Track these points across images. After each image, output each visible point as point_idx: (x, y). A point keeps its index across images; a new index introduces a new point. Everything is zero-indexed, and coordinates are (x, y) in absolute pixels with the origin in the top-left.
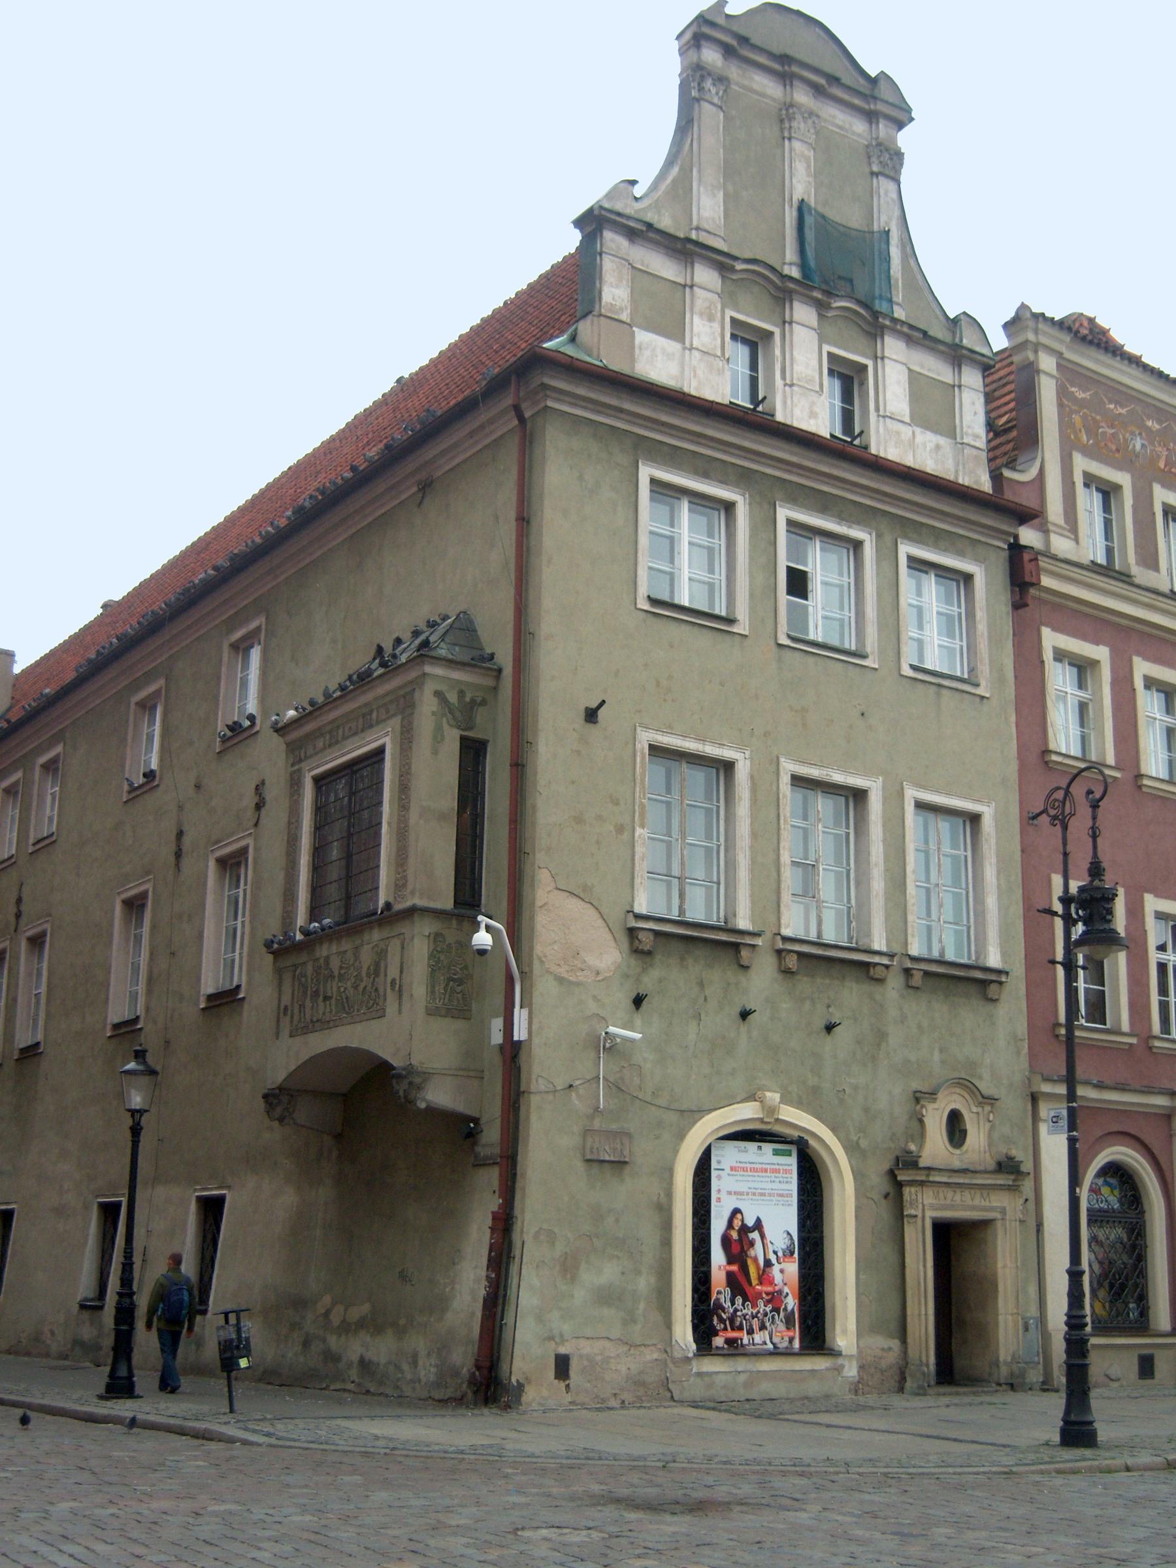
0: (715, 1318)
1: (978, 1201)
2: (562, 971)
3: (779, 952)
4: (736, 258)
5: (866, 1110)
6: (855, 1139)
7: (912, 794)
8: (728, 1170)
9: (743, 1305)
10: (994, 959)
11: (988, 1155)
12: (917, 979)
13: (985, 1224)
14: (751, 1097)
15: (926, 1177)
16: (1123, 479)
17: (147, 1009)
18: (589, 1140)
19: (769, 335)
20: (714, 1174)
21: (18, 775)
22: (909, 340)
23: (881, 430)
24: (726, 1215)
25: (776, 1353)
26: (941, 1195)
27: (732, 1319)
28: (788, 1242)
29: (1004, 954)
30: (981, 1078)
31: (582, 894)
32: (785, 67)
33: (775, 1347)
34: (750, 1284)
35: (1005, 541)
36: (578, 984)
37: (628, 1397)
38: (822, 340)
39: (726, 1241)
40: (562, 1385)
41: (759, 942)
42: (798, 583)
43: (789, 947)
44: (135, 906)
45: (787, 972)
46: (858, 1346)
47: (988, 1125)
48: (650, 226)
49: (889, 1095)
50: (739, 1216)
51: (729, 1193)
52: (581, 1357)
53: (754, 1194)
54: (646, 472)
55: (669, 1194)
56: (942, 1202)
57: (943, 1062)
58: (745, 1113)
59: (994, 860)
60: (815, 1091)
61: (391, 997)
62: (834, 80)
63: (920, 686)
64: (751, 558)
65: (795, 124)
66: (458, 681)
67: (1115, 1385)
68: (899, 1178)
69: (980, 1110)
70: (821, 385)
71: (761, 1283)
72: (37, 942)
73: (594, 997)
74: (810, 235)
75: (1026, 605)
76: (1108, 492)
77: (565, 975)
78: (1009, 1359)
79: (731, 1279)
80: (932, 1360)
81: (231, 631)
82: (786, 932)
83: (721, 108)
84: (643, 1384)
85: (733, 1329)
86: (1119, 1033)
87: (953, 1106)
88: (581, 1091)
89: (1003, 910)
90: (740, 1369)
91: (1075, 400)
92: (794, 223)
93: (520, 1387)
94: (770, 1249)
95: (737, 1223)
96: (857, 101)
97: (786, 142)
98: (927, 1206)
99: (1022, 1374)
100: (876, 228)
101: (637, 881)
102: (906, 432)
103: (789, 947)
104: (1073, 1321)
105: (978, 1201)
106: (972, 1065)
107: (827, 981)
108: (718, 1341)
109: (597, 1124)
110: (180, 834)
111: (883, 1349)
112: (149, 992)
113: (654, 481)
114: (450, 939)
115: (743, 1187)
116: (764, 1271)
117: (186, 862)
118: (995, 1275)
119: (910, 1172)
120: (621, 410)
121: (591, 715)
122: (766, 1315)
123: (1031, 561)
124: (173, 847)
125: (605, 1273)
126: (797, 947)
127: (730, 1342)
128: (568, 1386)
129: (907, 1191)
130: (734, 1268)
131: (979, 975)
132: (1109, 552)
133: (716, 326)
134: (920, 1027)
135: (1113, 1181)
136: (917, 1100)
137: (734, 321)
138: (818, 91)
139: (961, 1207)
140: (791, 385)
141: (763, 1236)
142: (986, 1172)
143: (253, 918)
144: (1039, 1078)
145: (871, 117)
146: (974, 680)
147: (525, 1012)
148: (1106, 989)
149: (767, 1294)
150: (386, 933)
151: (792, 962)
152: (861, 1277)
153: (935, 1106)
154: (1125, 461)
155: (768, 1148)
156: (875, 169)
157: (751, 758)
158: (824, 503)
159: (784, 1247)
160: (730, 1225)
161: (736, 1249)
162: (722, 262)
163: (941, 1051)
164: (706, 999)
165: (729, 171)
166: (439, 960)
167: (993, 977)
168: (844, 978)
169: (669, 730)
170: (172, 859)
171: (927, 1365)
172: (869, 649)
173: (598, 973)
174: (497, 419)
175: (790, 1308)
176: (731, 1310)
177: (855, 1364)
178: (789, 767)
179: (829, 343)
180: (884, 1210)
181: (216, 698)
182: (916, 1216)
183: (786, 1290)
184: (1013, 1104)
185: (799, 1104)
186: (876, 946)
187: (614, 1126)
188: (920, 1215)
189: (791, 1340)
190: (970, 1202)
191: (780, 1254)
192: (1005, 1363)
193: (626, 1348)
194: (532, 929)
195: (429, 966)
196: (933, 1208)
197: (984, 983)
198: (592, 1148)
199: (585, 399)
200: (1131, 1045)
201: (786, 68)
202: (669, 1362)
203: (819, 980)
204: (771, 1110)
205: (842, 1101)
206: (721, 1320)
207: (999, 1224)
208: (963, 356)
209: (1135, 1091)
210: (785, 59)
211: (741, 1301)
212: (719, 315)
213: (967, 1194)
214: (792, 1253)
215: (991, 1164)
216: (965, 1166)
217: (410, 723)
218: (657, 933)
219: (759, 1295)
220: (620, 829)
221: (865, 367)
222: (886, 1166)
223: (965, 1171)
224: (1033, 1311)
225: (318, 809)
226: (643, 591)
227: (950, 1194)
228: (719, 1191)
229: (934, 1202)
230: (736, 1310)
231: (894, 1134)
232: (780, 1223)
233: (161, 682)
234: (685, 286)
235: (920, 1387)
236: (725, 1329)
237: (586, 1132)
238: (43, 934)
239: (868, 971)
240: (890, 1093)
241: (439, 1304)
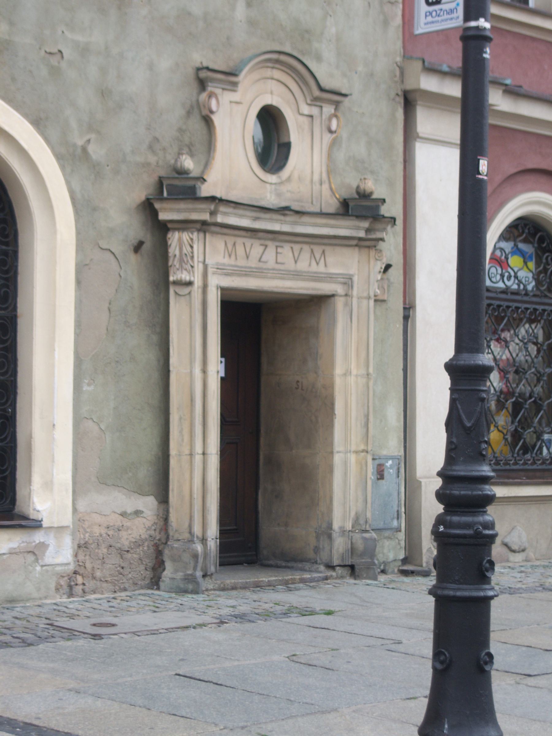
5: (104, 93)
6: (80, 142)
11: (326, 187)
13: (318, 302)
15: (211, 216)
26: (240, 250)
30: (319, 58)
46: (75, 510)
49: (151, 73)
56: (242, 262)
57: (252, 23)
67: (518, 558)
68: (163, 216)
69: (315, 111)
78: (349, 526)
80: (213, 530)
98: (212, 268)
99: (370, 551)
104: (459, 491)
106: (305, 34)
111: (123, 514)
118: (330, 387)
119: (182, 205)
129: (175, 239)
136: (202, 84)
139: (275, 272)
144: (418, 65)
152: (85, 388)
171: (204, 540)
180: (133, 273)
182: (190, 284)
184: (374, 108)
188: (198, 281)
190: (290, 265)
192: (343, 532)
196: (222, 270)
205: (55, 72)
207: (340, 303)
215: (331, 204)
216: (284, 204)
222: (140, 195)
223: (284, 210)
224: (393, 446)
227: (256, 249)
229: (226, 261)
231: (156, 139)
235: (190, 579)
240: (151, 67)
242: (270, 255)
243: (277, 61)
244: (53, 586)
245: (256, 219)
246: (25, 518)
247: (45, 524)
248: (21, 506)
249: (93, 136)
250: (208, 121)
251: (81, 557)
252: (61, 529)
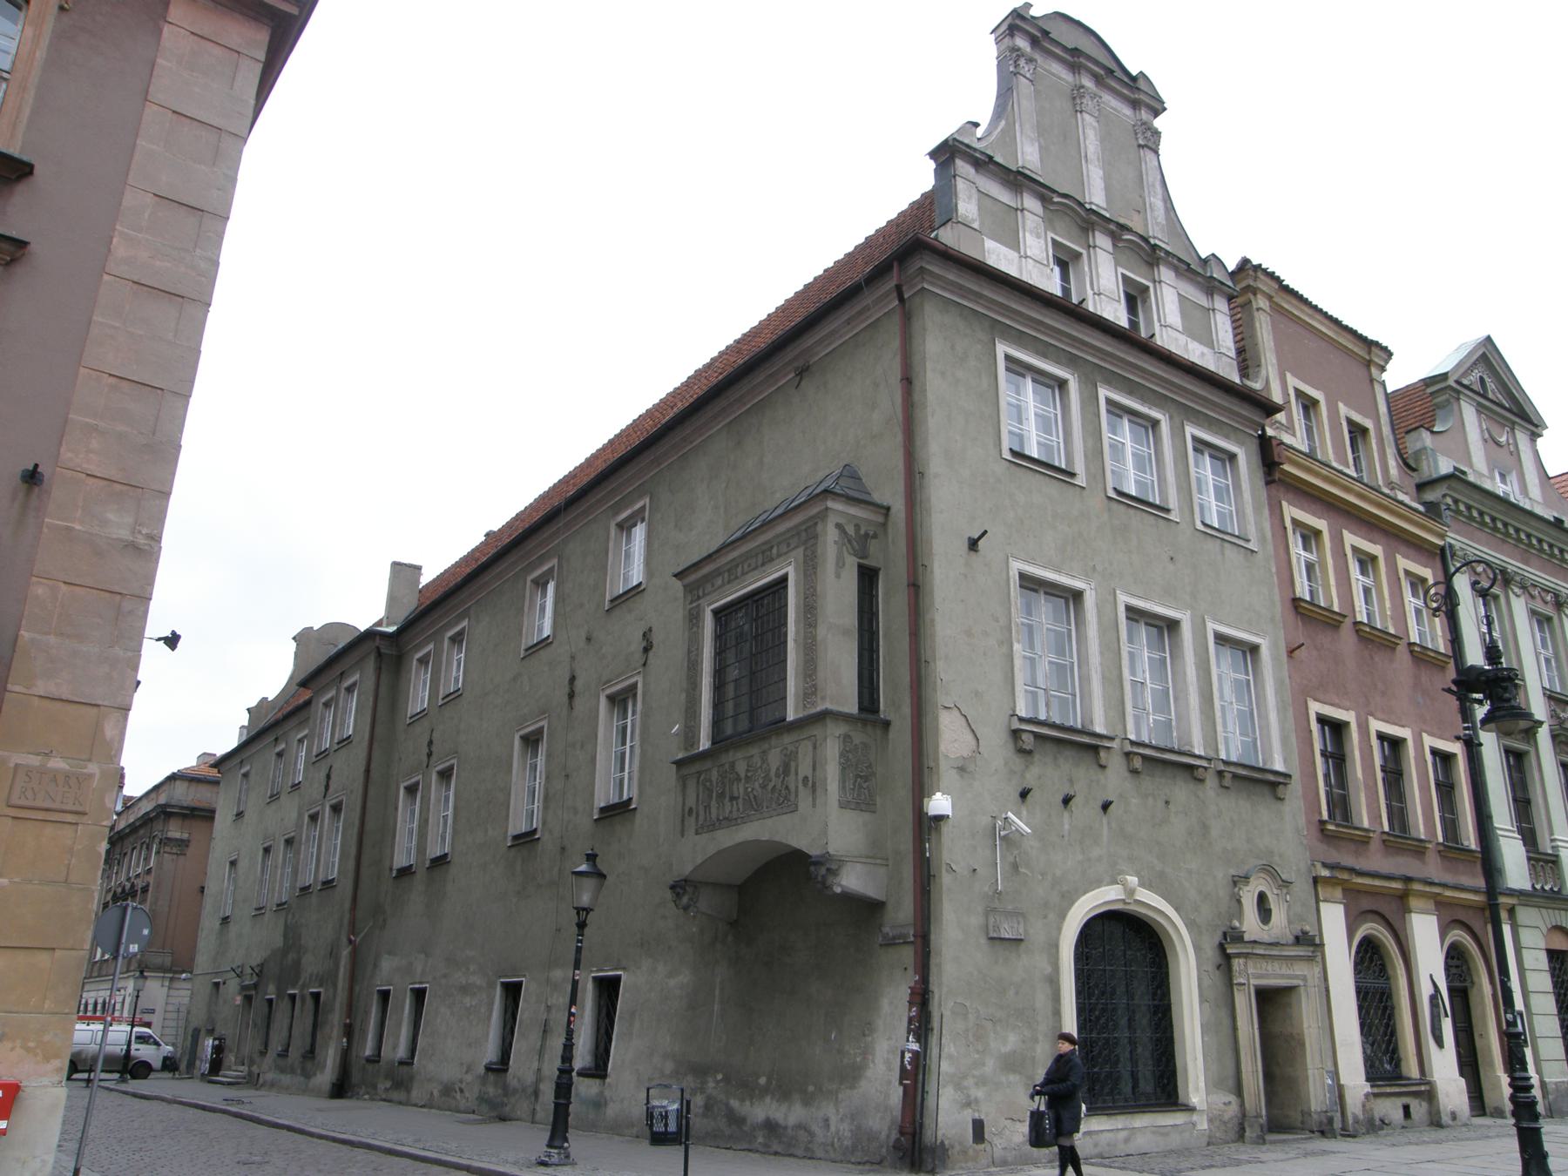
1: (1285, 971)
3: (1128, 755)
4: (1054, 191)
7: (1212, 626)
10: (1279, 766)
12: (1227, 781)
13: (1289, 990)
14: (1114, 882)
17: (544, 823)
18: (992, 920)
19: (1078, 256)
21: (431, 646)
22: (1176, 270)
29: (1285, 761)
32: (1075, 59)
38: (1117, 264)
44: (531, 741)
45: (1134, 772)
54: (1002, 349)
61: (804, 794)
63: (1209, 539)
72: (445, 775)
76: (1309, 405)
81: (617, 513)
87: (1261, 888)
89: (1282, 722)
98: (1251, 975)
102: (1183, 339)
103: (1136, 750)
105: (1285, 971)
110: (573, 679)
112: (546, 808)
113: (1008, 357)
114: (857, 741)
117: (577, 701)
118: (1301, 1034)
120: (980, 296)
121: (973, 544)
124: (567, 690)
126: (1141, 751)
129: (1237, 964)
131: (1271, 778)
134: (1232, 820)
136: (1235, 883)
137: (1054, 241)
139: (1275, 975)
143: (643, 741)
145: (1135, 104)
150: (794, 736)
158: (1131, 388)
165: (1042, 131)
166: (848, 760)
170: (565, 699)
174: (880, 302)
178: (1123, 599)
180: (1216, 978)
181: (605, 567)
184: (1302, 887)
194: (937, 728)
204: (1131, 892)
213: (1276, 964)
215: (1291, 939)
217: (814, 552)
218: (1036, 736)
223: (1276, 944)
225: (718, 637)
226: (1005, 446)
233: (555, 561)
238: (451, 768)
241: (851, 1074)
248: (1182, 1099)
250: (1239, 901)
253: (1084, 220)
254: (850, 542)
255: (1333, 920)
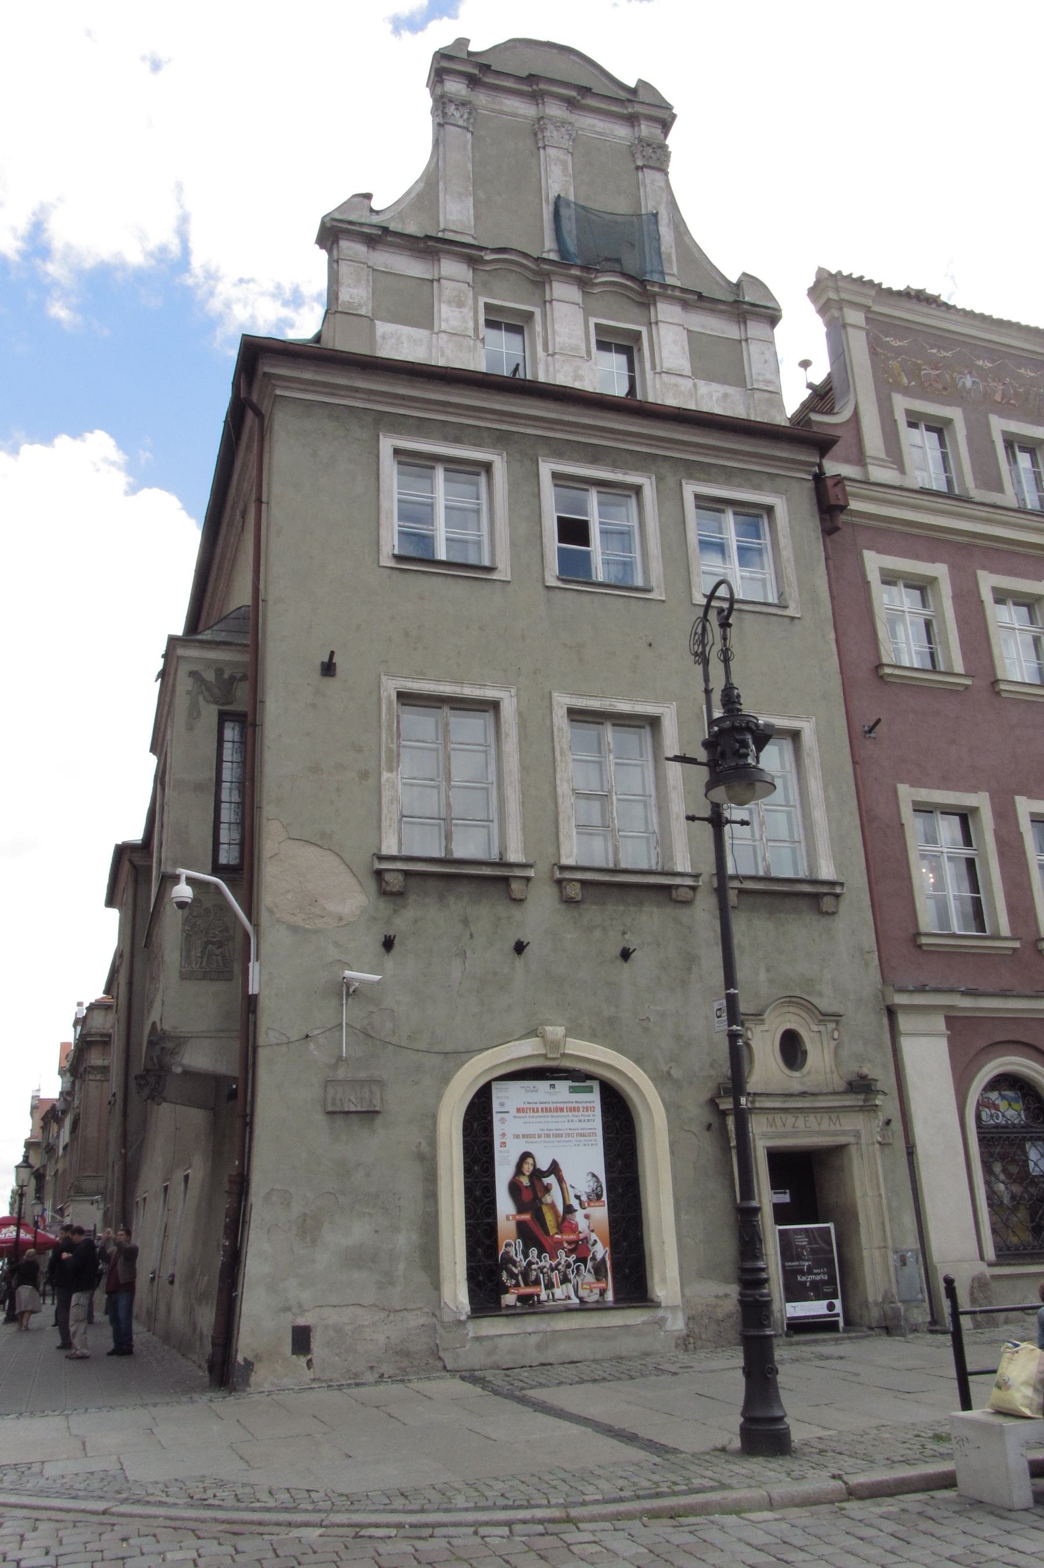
0: (504, 1276)
1: (825, 1125)
2: (298, 920)
3: (559, 882)
5: (678, 1038)
6: (665, 1069)
8: (513, 1112)
9: (539, 1257)
10: (826, 871)
11: (835, 1076)
13: (839, 1149)
14: (532, 1033)
16: (954, 413)
18: (331, 1092)
19: (529, 316)
20: (496, 1118)
22: (685, 304)
23: (658, 385)
24: (514, 1159)
25: (583, 1307)
26: (779, 1122)
27: (525, 1273)
28: (593, 1184)
29: (839, 867)
30: (820, 995)
31: (322, 841)
33: (581, 1299)
34: (547, 1232)
35: (808, 472)
36: (316, 932)
37: (387, 1369)
38: (587, 313)
39: (514, 1188)
40: (303, 1360)
41: (531, 873)
42: (574, 531)
43: (568, 875)
46: (683, 1295)
47: (833, 1043)
48: (385, 230)
50: (530, 1160)
51: (517, 1136)
52: (326, 1327)
53: (548, 1136)
54: (387, 444)
55: (433, 1143)
56: (781, 1129)
57: (771, 981)
58: (524, 1050)
59: (819, 773)
60: (612, 1021)
62: (585, 91)
64: (511, 510)
65: (547, 134)
66: (216, 661)
69: (822, 1028)
70: (589, 352)
71: (560, 1231)
73: (336, 944)
74: (569, 226)
75: (837, 529)
77: (301, 923)
78: (880, 1299)
79: (522, 1229)
82: (565, 861)
83: (467, 129)
84: (408, 1354)
85: (527, 1284)
86: (998, 938)
88: (321, 1040)
90: (530, 1330)
91: (891, 348)
92: (551, 216)
93: (249, 1365)
94: (571, 1193)
95: (528, 1168)
96: (614, 108)
97: (542, 151)
100: (643, 212)
101: (385, 824)
102: (686, 384)
103: (568, 875)
105: (825, 1125)
107: (621, 908)
108: (509, 1299)
109: (341, 1073)
111: (717, 1297)
113: (397, 452)
115: (534, 1129)
116: (564, 1218)
118: (854, 1205)
120: (357, 390)
121: (328, 669)
122: (568, 1266)
123: (836, 485)
125: (358, 1232)
126: (578, 876)
127: (523, 1299)
128: (309, 1363)
130: (526, 1217)
132: (949, 482)
133: (468, 312)
135: (1009, 1094)
137: (488, 307)
138: (571, 103)
139: (805, 1133)
140: (552, 355)
141: (561, 1180)
142: (834, 1093)
144: (891, 988)
145: (632, 120)
146: (783, 604)
147: (257, 964)
148: (982, 895)
149: (569, 1243)
151: (574, 891)
152: (683, 1217)
153: (765, 1027)
154: (952, 394)
155: (563, 1086)
156: (640, 163)
157: (518, 696)
158: (595, 455)
159: (589, 1190)
160: (519, 1170)
161: (527, 1197)
162: (471, 255)
163: (768, 971)
164: (471, 936)
167: (824, 889)
168: (641, 903)
169: (421, 676)
172: (654, 583)
173: (341, 919)
175: (599, 1257)
176: (524, 1264)
177: (680, 1315)
179: (595, 316)
183: (594, 1236)
184: (866, 1021)
185: (593, 1037)
186: (679, 869)
187: (362, 1075)
189: (603, 1292)
190: (815, 1127)
191: (584, 1198)
192: (876, 1304)
193: (383, 1315)
195: (183, 931)
196: (765, 1136)
197: (816, 897)
198: (334, 1100)
199: (314, 383)
200: (1014, 949)
201: (534, 87)
202: (438, 1327)
203: (610, 908)
204: (555, 1045)
206: (512, 1275)
207: (853, 1149)
208: (747, 312)
209: (1019, 996)
210: (532, 79)
211: (536, 1252)
212: (470, 302)
213: (812, 1118)
214: (599, 1197)
215: (840, 1085)
218: (407, 874)
219: (559, 1244)
220: (364, 775)
221: (640, 332)
222: (706, 1095)
223: (803, 1094)
224: (911, 1242)
227: (790, 1119)
228: (504, 1135)
229: (769, 1129)
230: (530, 1263)
231: (715, 1060)
232: (583, 1164)
234: (432, 281)
236: (517, 1285)
237: (327, 1083)
239: (671, 892)
242: (800, 1122)
243: (790, 1002)
244: (673, 1345)
245: (785, 1102)
246: (652, 1301)
247: (663, 1305)
248: (650, 1295)
249: (673, 1064)
251: (691, 1326)
252: (674, 1308)
253: (534, 272)
254: (208, 689)
255: (927, 1058)
